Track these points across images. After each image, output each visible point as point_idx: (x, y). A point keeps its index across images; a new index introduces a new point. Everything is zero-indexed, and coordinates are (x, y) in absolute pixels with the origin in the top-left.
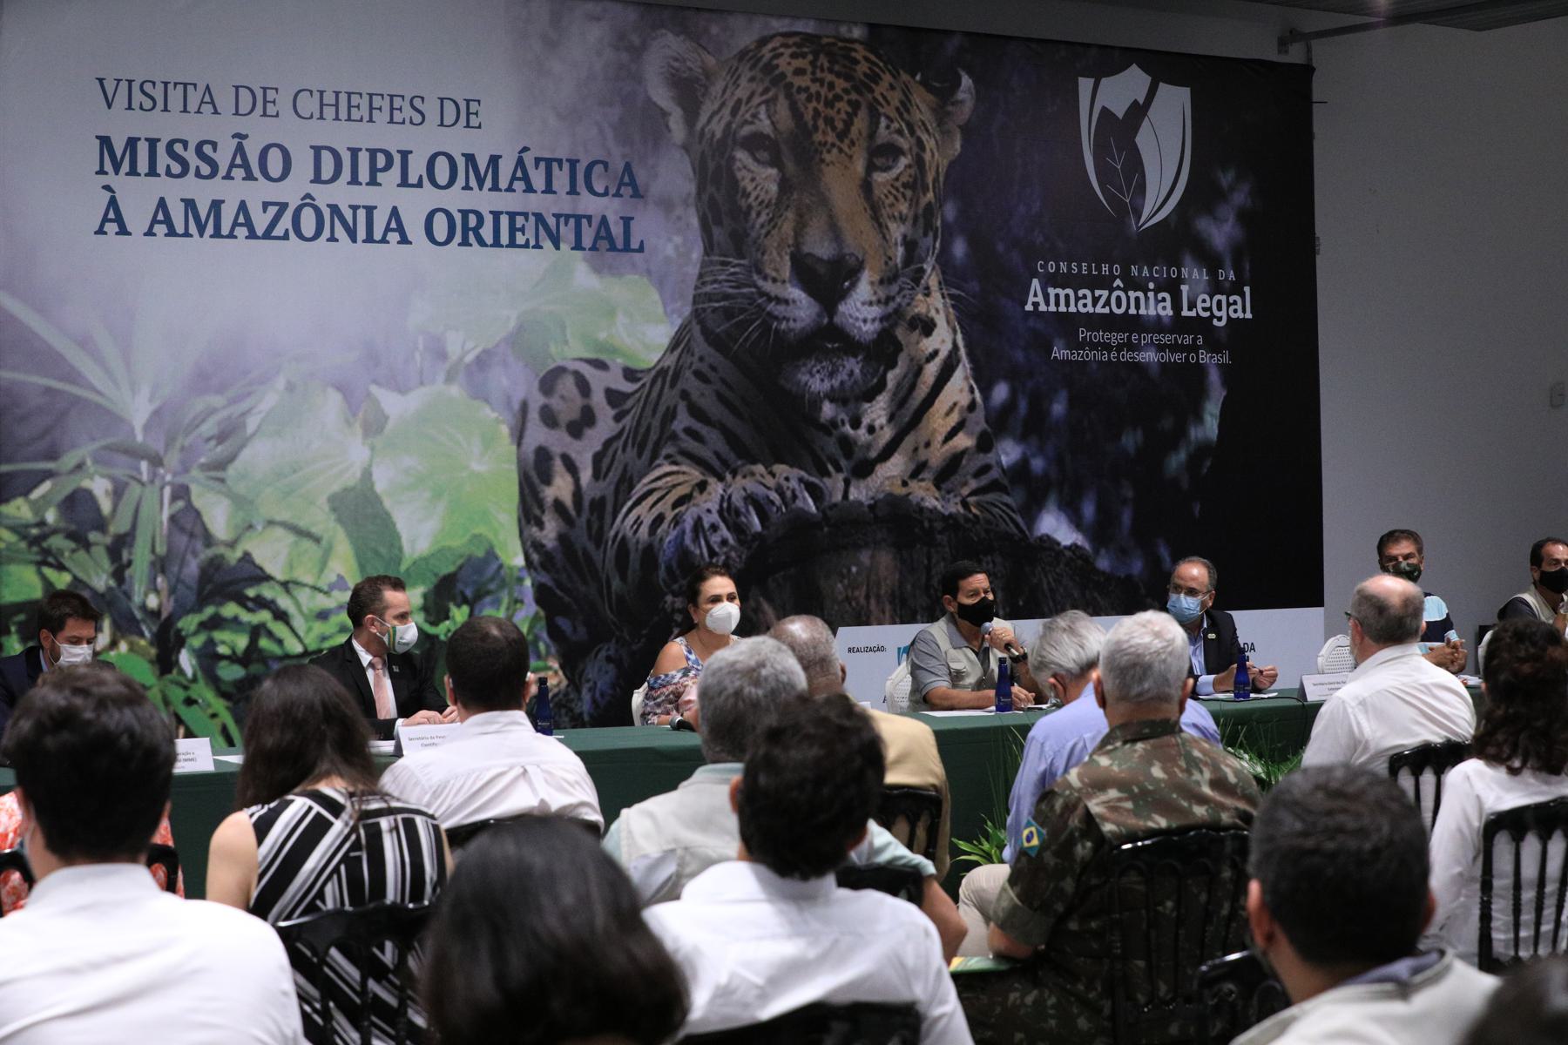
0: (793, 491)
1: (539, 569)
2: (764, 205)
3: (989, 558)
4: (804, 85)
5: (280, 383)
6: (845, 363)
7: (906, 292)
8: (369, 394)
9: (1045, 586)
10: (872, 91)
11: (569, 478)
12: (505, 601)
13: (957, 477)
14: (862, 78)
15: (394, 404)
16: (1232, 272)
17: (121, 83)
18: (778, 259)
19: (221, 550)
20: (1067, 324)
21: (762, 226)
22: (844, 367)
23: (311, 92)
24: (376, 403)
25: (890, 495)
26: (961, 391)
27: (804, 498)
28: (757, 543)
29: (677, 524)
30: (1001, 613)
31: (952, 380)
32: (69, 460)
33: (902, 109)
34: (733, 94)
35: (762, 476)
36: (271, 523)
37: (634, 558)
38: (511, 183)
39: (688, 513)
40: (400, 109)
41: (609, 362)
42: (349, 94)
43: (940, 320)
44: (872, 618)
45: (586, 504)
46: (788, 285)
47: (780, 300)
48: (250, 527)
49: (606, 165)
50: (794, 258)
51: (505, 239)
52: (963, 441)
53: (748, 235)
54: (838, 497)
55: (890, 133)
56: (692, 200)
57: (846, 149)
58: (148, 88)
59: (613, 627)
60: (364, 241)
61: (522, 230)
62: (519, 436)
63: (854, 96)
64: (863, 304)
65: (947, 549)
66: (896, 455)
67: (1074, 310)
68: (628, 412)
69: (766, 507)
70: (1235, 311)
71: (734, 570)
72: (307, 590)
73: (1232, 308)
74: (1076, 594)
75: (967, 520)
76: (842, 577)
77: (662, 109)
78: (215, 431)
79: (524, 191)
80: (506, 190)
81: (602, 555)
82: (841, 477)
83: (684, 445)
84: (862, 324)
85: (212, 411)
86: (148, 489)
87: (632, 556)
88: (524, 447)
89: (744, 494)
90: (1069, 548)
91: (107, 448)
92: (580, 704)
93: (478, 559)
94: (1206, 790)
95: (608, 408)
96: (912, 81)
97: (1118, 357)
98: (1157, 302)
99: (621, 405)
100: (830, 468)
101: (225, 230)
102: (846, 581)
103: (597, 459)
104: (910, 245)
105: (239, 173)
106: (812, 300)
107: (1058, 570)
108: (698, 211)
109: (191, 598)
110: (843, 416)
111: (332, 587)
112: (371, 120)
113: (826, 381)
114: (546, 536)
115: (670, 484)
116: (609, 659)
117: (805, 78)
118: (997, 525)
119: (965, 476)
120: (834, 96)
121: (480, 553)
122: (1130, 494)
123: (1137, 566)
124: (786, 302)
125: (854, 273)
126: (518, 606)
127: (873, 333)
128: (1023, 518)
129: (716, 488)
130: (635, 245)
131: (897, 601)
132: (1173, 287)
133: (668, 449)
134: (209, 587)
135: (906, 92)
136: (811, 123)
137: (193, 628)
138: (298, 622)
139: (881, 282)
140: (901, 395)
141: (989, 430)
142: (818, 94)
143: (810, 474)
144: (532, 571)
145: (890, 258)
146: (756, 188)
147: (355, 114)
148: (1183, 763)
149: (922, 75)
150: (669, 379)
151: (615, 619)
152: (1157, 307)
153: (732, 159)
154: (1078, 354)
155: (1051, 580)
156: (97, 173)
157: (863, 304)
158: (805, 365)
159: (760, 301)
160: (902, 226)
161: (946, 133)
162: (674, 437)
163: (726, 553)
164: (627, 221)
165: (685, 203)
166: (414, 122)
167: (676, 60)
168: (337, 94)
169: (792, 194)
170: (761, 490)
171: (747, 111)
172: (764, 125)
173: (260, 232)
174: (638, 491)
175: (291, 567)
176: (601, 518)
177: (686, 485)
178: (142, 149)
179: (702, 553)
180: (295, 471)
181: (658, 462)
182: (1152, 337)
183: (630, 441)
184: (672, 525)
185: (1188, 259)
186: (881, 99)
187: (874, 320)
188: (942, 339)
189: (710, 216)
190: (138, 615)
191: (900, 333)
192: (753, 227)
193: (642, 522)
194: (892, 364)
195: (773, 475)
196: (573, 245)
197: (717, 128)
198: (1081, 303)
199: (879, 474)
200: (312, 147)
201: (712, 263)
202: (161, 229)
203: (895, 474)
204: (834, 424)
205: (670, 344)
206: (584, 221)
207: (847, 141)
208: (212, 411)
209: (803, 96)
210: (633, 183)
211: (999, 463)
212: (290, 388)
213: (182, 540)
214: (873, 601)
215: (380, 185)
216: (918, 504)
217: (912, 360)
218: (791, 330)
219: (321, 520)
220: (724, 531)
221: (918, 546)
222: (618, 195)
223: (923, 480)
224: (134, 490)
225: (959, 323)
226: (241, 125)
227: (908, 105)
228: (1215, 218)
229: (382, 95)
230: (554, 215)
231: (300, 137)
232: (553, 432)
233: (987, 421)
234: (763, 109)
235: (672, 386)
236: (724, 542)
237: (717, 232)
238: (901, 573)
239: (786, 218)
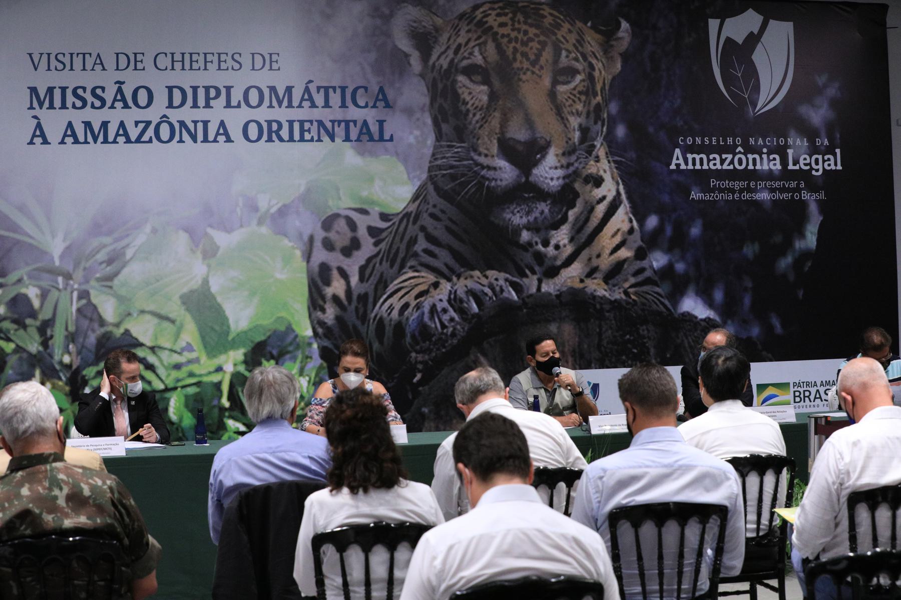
0: (501, 287)
1: (323, 337)
2: (478, 109)
3: (644, 327)
4: (506, 33)
5: (148, 229)
6: (538, 206)
7: (582, 160)
8: (206, 234)
9: (687, 345)
10: (555, 34)
11: (342, 282)
12: (300, 357)
13: (621, 276)
14: (549, 26)
15: (221, 239)
16: (826, 140)
17: (43, 55)
18: (489, 142)
19: (110, 328)
20: (702, 177)
21: (477, 122)
22: (537, 208)
23: (166, 54)
24: (211, 239)
25: (572, 288)
26: (623, 221)
27: (509, 291)
28: (476, 319)
31: (616, 214)
32: (12, 277)
33: (577, 45)
34: (455, 40)
35: (479, 278)
36: (143, 312)
37: (389, 331)
38: (301, 102)
39: (426, 302)
40: (225, 61)
41: (369, 210)
42: (191, 54)
43: (607, 177)
45: (355, 297)
46: (496, 158)
47: (489, 168)
48: (129, 314)
49: (366, 88)
50: (499, 140)
51: (297, 136)
52: (624, 253)
53: (467, 128)
54: (534, 290)
55: (569, 61)
56: (427, 108)
57: (537, 72)
58: (60, 57)
60: (202, 142)
61: (309, 131)
62: (308, 257)
63: (542, 38)
64: (551, 168)
65: (613, 322)
66: (575, 263)
67: (707, 168)
68: (383, 240)
69: (482, 297)
70: (829, 165)
71: (459, 337)
72: (167, 352)
73: (826, 163)
75: (628, 303)
77: (404, 52)
78: (106, 258)
79: (310, 107)
80: (297, 107)
81: (366, 330)
82: (535, 277)
83: (423, 260)
84: (550, 181)
85: (105, 246)
86: (63, 293)
87: (387, 328)
88: (311, 263)
89: (465, 289)
90: (704, 320)
91: (35, 270)
93: (282, 332)
95: (369, 238)
96: (584, 26)
97: (740, 197)
98: (769, 160)
99: (378, 236)
100: (527, 271)
101: (111, 139)
103: (362, 270)
104: (585, 131)
105: (119, 105)
106: (513, 167)
107: (696, 334)
108: (431, 114)
109: (92, 357)
111: (183, 350)
112: (206, 69)
113: (524, 218)
114: (327, 317)
115: (413, 284)
117: (507, 28)
120: (528, 38)
121: (282, 328)
122: (749, 284)
123: (755, 331)
124: (495, 169)
125: (543, 149)
126: (309, 360)
127: (558, 186)
128: (670, 302)
129: (446, 286)
130: (387, 137)
132: (782, 151)
133: (412, 262)
134: (103, 351)
135: (580, 34)
136: (511, 57)
137: (93, 374)
138: (161, 371)
139: (564, 154)
140: (578, 225)
141: (644, 245)
142: (516, 38)
143: (513, 276)
144: (318, 338)
145: (570, 139)
146: (472, 98)
147: (195, 66)
149: (592, 23)
150: (411, 219)
151: (376, 368)
152: (770, 164)
153: (455, 81)
154: (710, 196)
155: (691, 340)
156: (29, 109)
157: (551, 168)
158: (509, 208)
159: (476, 169)
160: (578, 118)
161: (610, 59)
162: (416, 255)
163: (453, 326)
164: (381, 123)
165: (422, 109)
166: (235, 68)
167: (415, 22)
168: (183, 54)
169: (498, 101)
170: (478, 287)
171: (465, 51)
172: (478, 59)
173: (133, 139)
175: (156, 339)
178: (57, 94)
179: (436, 327)
180: (158, 281)
181: (404, 270)
182: (765, 184)
183: (385, 258)
184: (415, 310)
185: (792, 133)
186: (562, 40)
187: (558, 178)
188: (609, 189)
189: (440, 118)
190: (58, 367)
191: (577, 186)
192: (470, 123)
193: (393, 308)
194: (573, 206)
195: (487, 277)
196: (344, 139)
197: (444, 63)
198: (711, 163)
199: (563, 275)
200: (166, 87)
201: (441, 146)
202: (69, 140)
203: (574, 274)
204: (530, 244)
205: (413, 197)
206: (352, 124)
207: (537, 67)
208: (105, 246)
209: (506, 40)
210: (385, 99)
211: (651, 267)
212: (154, 231)
213: (85, 323)
215: (212, 107)
216: (592, 294)
217: (586, 203)
218: (500, 186)
219: (176, 309)
220: (452, 313)
221: (592, 320)
222: (374, 106)
223: (595, 278)
224: (54, 294)
225: (621, 179)
226: (120, 76)
227: (582, 42)
228: (813, 106)
229: (213, 54)
230: (330, 121)
231: (158, 82)
232: (331, 254)
233: (642, 240)
234: (476, 50)
235: (414, 223)
236: (452, 320)
237: (445, 127)
238: (579, 336)
239: (494, 116)
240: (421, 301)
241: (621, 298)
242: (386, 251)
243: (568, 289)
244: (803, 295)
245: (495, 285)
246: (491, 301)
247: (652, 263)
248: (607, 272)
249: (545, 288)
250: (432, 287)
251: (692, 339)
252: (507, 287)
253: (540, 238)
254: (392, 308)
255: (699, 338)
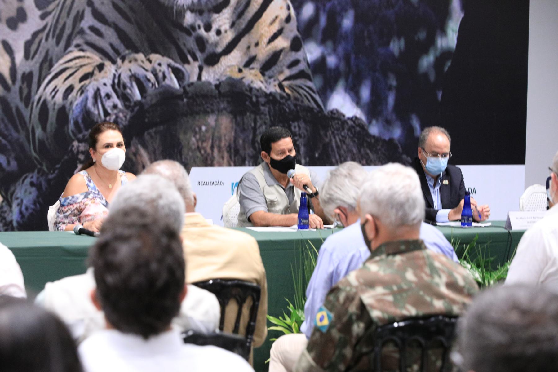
3: (296, 124)
9: (334, 144)
25: (230, 78)
26: (281, 8)
27: (171, 78)
29: (82, 92)
30: (303, 161)
35: (143, 62)
37: (52, 116)
44: (215, 162)
45: (19, 76)
52: (282, 43)
54: (194, 78)
59: (35, 162)
65: (268, 117)
69: (145, 84)
71: (121, 126)
74: (355, 151)
75: (282, 97)
76: (196, 133)
89: (130, 74)
90: (351, 119)
92: (11, 215)
94: (444, 290)
100: (190, 58)
102: (198, 136)
103: (28, 45)
107: (343, 134)
110: (199, 22)
115: (78, 65)
116: (32, 184)
118: (302, 102)
119: (282, 67)
122: (393, 82)
123: (397, 133)
128: (320, 97)
129: (110, 69)
131: (232, 151)
133: (78, 40)
141: (299, 36)
143: (176, 62)
148: (427, 270)
151: (37, 157)
162: (82, 32)
170: (140, 72)
174: (56, 69)
176: (29, 86)
177: (89, 66)
179: (99, 114)
193: (58, 91)
195: (150, 62)
199: (223, 63)
204: (193, 28)
211: (305, 59)
214: (216, 150)
220: (115, 99)
221: (248, 114)
223: (253, 68)
233: (298, 30)
236: (115, 107)
240: (85, 84)
241: (276, 91)
242: (53, 26)
243: (227, 79)
244: (442, 97)
245: (158, 71)
246: (154, 88)
247: (306, 55)
248: (264, 62)
249: (205, 77)
250: (97, 69)
251: (339, 138)
252: (169, 73)
253: (202, 21)
254: (56, 90)
255: (346, 138)
